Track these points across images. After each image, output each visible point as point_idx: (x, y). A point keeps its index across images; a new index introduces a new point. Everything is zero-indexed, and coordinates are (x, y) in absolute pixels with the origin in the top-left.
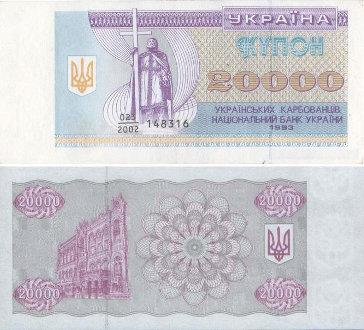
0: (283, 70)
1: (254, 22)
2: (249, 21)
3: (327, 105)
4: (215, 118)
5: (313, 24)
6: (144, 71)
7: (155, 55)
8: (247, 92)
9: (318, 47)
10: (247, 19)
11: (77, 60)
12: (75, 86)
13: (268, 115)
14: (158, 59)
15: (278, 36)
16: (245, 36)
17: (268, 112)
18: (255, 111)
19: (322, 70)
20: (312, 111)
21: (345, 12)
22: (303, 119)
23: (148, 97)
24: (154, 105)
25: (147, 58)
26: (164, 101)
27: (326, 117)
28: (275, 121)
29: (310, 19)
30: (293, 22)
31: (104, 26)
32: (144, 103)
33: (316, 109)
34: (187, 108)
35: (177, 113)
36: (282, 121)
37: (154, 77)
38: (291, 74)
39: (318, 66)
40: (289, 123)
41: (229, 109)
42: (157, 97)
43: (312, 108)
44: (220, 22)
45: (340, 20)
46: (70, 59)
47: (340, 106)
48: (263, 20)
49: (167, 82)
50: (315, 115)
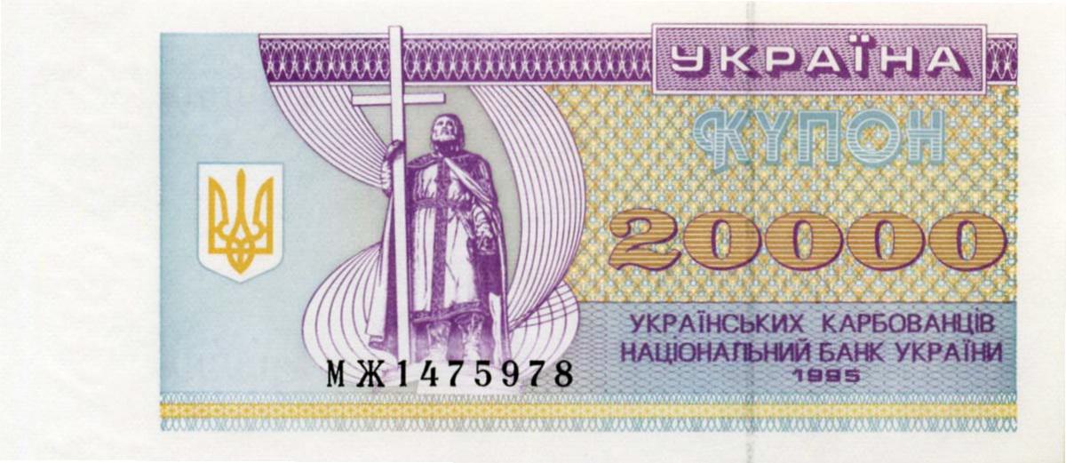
0: (828, 209)
1: (744, 68)
2: (730, 65)
3: (957, 311)
4: (629, 347)
5: (915, 73)
6: (423, 210)
7: (456, 162)
8: (725, 273)
9: (928, 142)
10: (725, 59)
11: (226, 176)
12: (220, 251)
13: (785, 338)
14: (463, 175)
15: (815, 108)
16: (716, 109)
17: (785, 330)
18: (745, 328)
19: (942, 210)
20: (914, 327)
21: (1007, 40)
22: (889, 353)
23: (433, 285)
24: (452, 308)
25: (431, 173)
26: (480, 297)
27: (952, 346)
28: (804, 356)
29: (908, 59)
30: (859, 67)
31: (307, 78)
32: (423, 302)
33: (923, 323)
34: (549, 317)
35: (519, 332)
36: (827, 356)
37: (451, 227)
38: (850, 220)
39: (930, 197)
40: (845, 365)
41: (669, 319)
42: (461, 285)
43: (914, 319)
44: (645, 67)
45: (996, 65)
46: (206, 172)
47: (994, 314)
48: (771, 64)
49: (490, 241)
50: (920, 338)
